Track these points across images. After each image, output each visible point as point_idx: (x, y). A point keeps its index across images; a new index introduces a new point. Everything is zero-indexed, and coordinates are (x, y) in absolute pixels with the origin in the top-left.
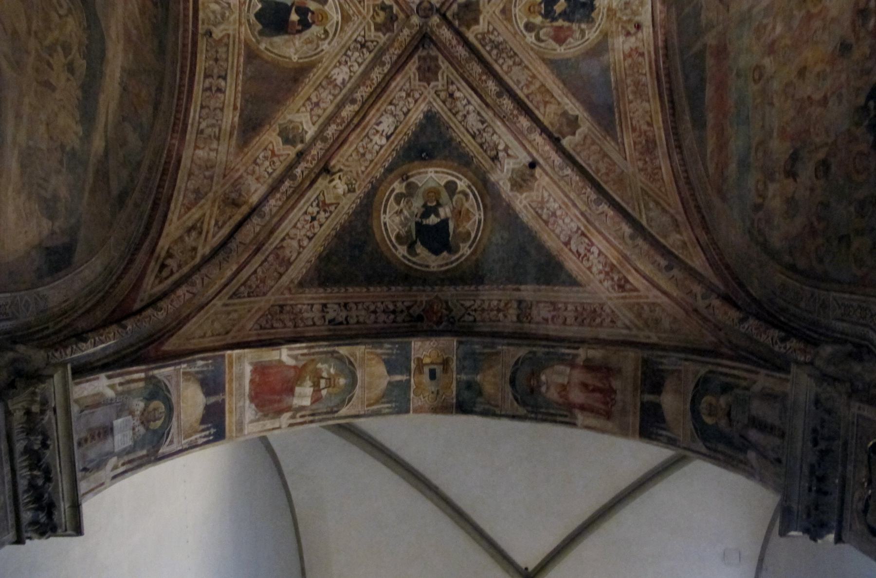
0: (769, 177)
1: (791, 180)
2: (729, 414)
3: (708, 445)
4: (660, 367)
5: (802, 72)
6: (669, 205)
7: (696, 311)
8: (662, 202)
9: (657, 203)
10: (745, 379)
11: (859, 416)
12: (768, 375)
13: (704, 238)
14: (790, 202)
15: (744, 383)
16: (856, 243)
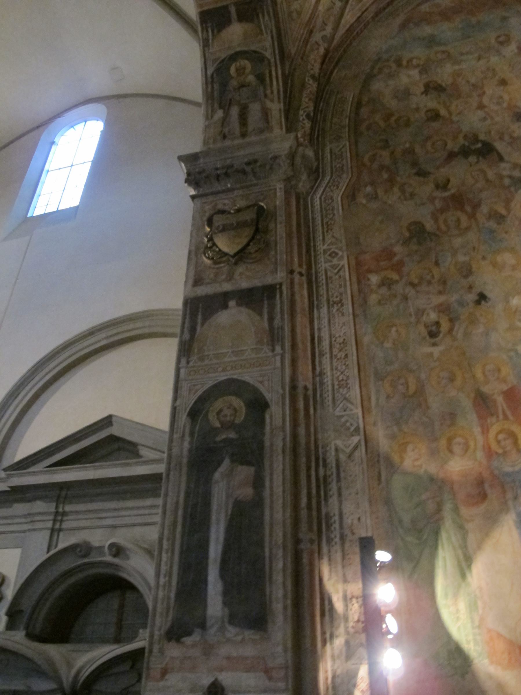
0: (424, 70)
1: (423, 89)
2: (243, 86)
3: (215, 75)
4: (260, 15)
5: (503, 82)
7: (311, 32)
10: (272, 92)
11: (275, 189)
12: (280, 110)
13: (369, 15)
14: (407, 93)
15: (268, 92)
16: (385, 154)
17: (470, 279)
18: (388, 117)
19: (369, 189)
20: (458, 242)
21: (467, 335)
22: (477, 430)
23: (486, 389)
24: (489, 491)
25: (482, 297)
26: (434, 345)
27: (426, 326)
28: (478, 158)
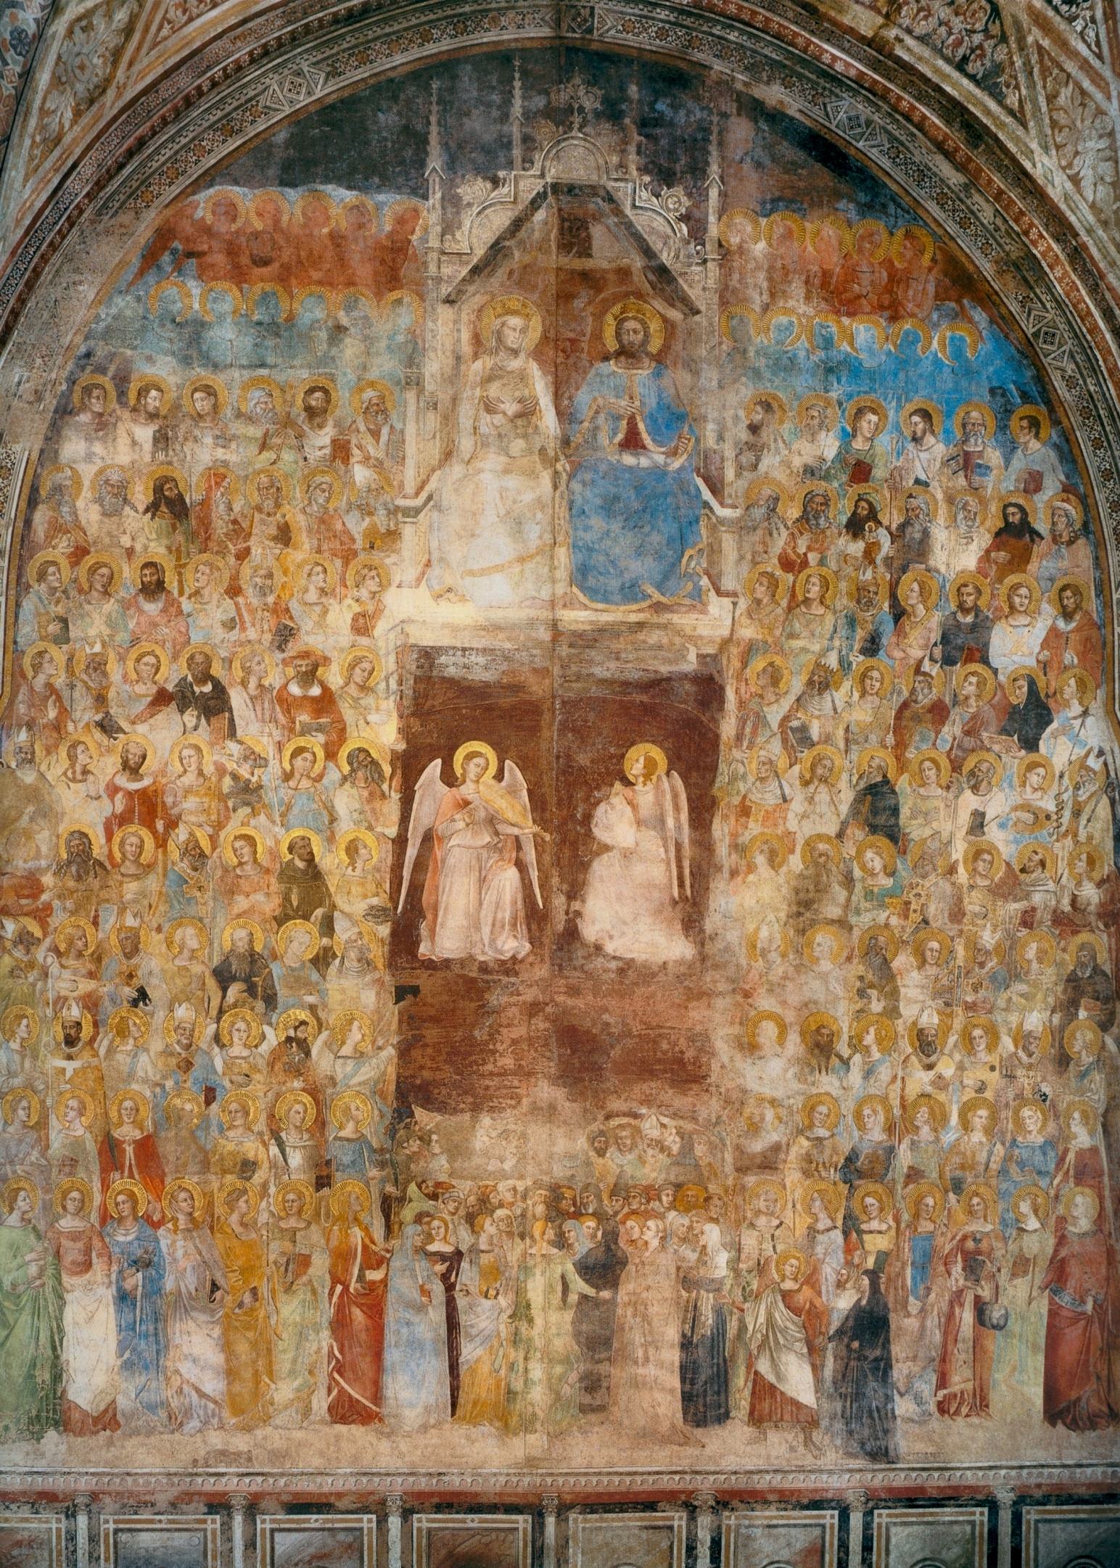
6: (131, 64)
8: (137, 37)
9: (128, 31)
17: (133, 961)
18: (79, 553)
19: (23, 736)
20: (131, 888)
21: (111, 1051)
22: (96, 1185)
23: (116, 1134)
24: (95, 1260)
25: (142, 995)
26: (70, 1058)
27: (64, 1027)
28: (198, 718)
